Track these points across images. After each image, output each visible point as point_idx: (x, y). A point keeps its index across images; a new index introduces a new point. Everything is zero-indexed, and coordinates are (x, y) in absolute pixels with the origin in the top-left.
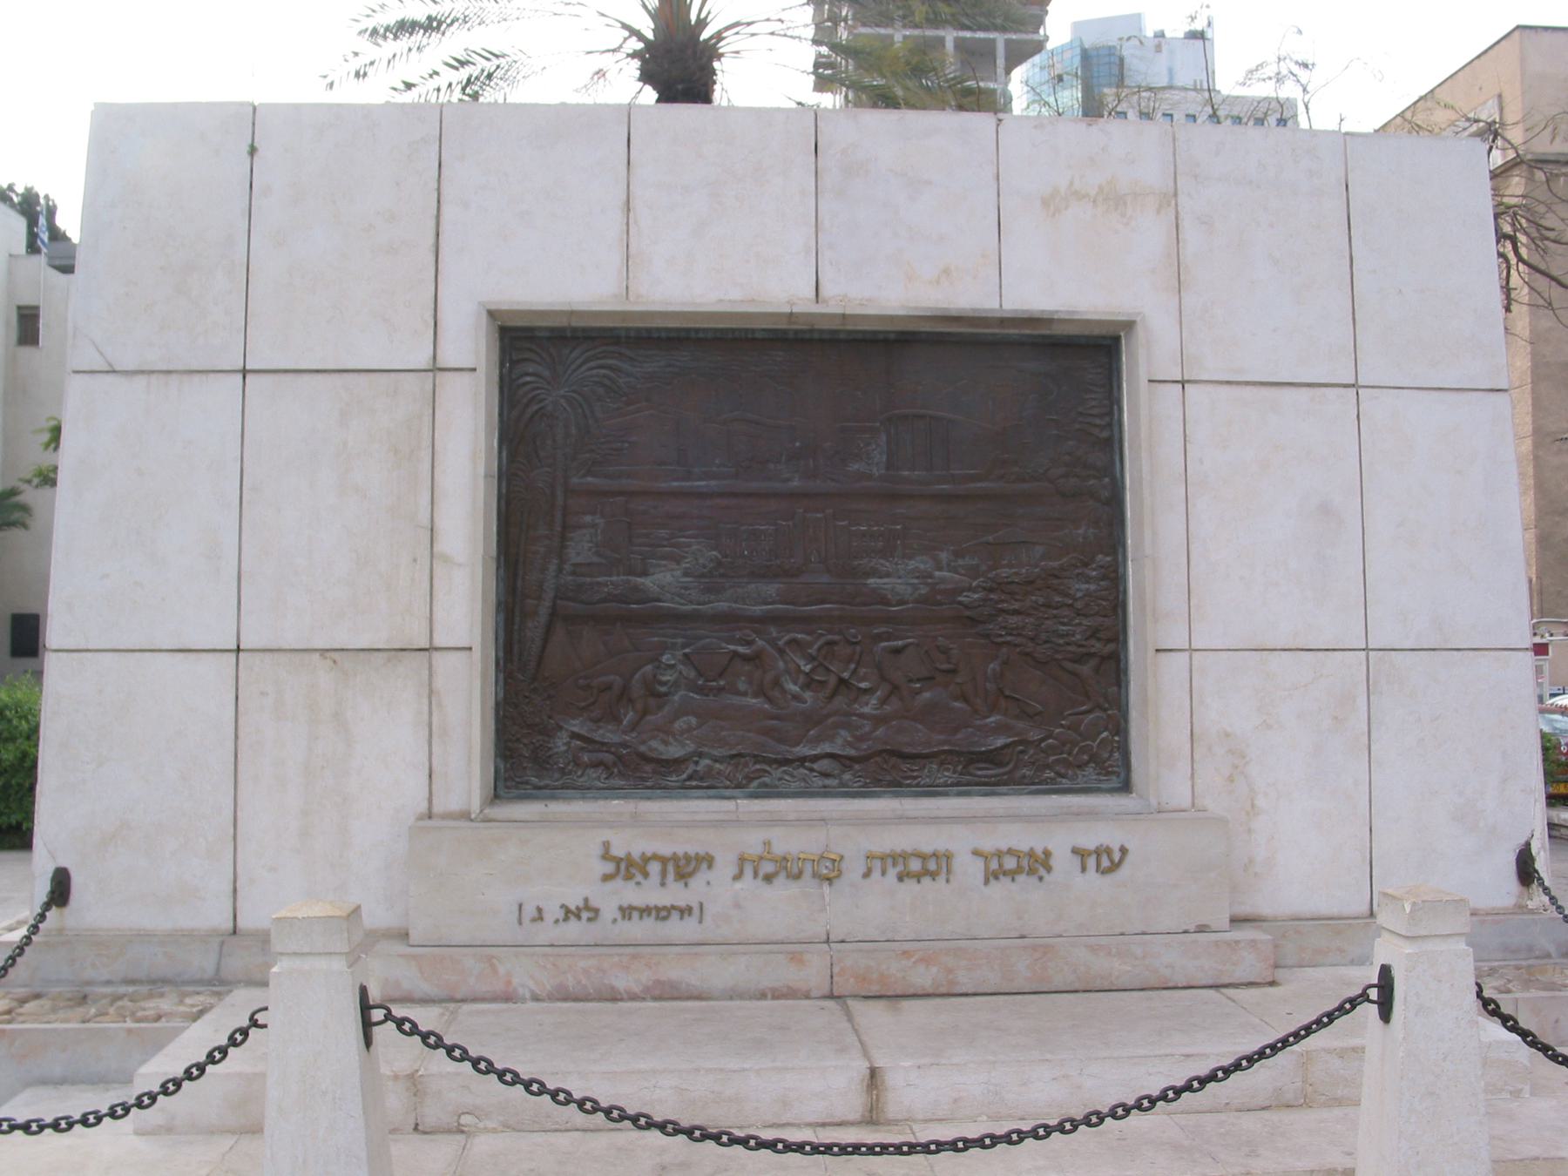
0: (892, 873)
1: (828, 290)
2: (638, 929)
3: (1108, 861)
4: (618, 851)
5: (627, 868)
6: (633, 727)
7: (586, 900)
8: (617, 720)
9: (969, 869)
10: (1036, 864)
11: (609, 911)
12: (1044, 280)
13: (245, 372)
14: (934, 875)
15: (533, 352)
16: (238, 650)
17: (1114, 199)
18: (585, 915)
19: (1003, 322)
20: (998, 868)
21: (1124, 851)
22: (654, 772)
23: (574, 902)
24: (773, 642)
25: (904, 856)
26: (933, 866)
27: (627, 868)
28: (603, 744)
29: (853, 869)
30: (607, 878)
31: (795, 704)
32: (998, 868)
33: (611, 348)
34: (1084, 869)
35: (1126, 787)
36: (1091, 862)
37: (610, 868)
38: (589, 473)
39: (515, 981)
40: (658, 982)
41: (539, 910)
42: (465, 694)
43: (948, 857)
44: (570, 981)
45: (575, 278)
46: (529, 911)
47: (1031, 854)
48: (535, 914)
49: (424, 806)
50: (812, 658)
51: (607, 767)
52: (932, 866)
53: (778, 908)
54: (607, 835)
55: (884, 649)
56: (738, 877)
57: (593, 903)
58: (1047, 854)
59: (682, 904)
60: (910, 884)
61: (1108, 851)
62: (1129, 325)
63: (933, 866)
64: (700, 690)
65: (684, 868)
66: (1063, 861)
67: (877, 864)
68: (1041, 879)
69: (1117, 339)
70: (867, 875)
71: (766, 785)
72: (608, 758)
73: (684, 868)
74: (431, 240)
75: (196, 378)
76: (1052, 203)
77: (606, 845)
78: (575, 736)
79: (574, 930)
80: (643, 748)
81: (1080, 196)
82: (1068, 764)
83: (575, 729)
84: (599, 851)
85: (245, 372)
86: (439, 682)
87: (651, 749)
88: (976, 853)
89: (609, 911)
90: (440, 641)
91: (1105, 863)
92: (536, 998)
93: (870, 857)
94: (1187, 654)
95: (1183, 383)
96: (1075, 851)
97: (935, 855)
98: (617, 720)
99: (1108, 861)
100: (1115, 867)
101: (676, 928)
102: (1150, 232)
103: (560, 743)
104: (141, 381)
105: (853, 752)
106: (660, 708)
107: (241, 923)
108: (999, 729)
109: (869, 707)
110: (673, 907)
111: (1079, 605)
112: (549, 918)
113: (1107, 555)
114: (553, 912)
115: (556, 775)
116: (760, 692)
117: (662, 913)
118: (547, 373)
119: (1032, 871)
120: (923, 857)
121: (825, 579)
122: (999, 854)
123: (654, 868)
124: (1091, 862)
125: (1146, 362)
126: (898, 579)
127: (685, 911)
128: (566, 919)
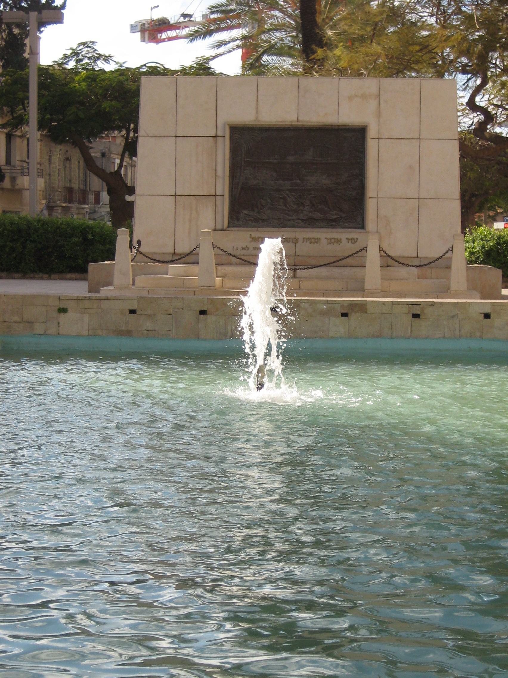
0: (308, 242)
1: (300, 119)
3: (354, 241)
4: (253, 236)
8: (254, 211)
9: (324, 242)
10: (338, 241)
11: (251, 249)
12: (348, 116)
13: (176, 136)
14: (316, 242)
16: (175, 195)
17: (364, 97)
19: (338, 126)
20: (331, 241)
21: (357, 239)
23: (244, 246)
24: (287, 195)
25: (311, 239)
26: (317, 241)
29: (300, 241)
30: (251, 242)
32: (331, 241)
36: (350, 241)
37: (251, 239)
43: (320, 239)
45: (246, 116)
46: (235, 248)
47: (337, 239)
49: (214, 228)
50: (296, 198)
52: (316, 240)
54: (251, 233)
57: (248, 246)
58: (341, 239)
60: (312, 244)
61: (354, 239)
62: (367, 126)
63: (317, 241)
66: (344, 241)
67: (305, 240)
70: (303, 242)
72: (253, 219)
74: (215, 108)
75: (166, 138)
76: (350, 98)
81: (356, 96)
82: (350, 222)
84: (249, 236)
85: (176, 136)
86: (218, 203)
88: (326, 238)
89: (251, 249)
90: (217, 194)
91: (353, 241)
93: (304, 238)
94: (376, 199)
95: (378, 139)
96: (347, 239)
97: (317, 239)
98: (254, 211)
99: (354, 241)
100: (355, 242)
102: (373, 104)
103: (242, 215)
104: (154, 138)
112: (239, 250)
114: (240, 248)
116: (285, 205)
119: (337, 243)
120: (315, 239)
121: (299, 181)
122: (331, 239)
124: (350, 241)
125: (372, 133)
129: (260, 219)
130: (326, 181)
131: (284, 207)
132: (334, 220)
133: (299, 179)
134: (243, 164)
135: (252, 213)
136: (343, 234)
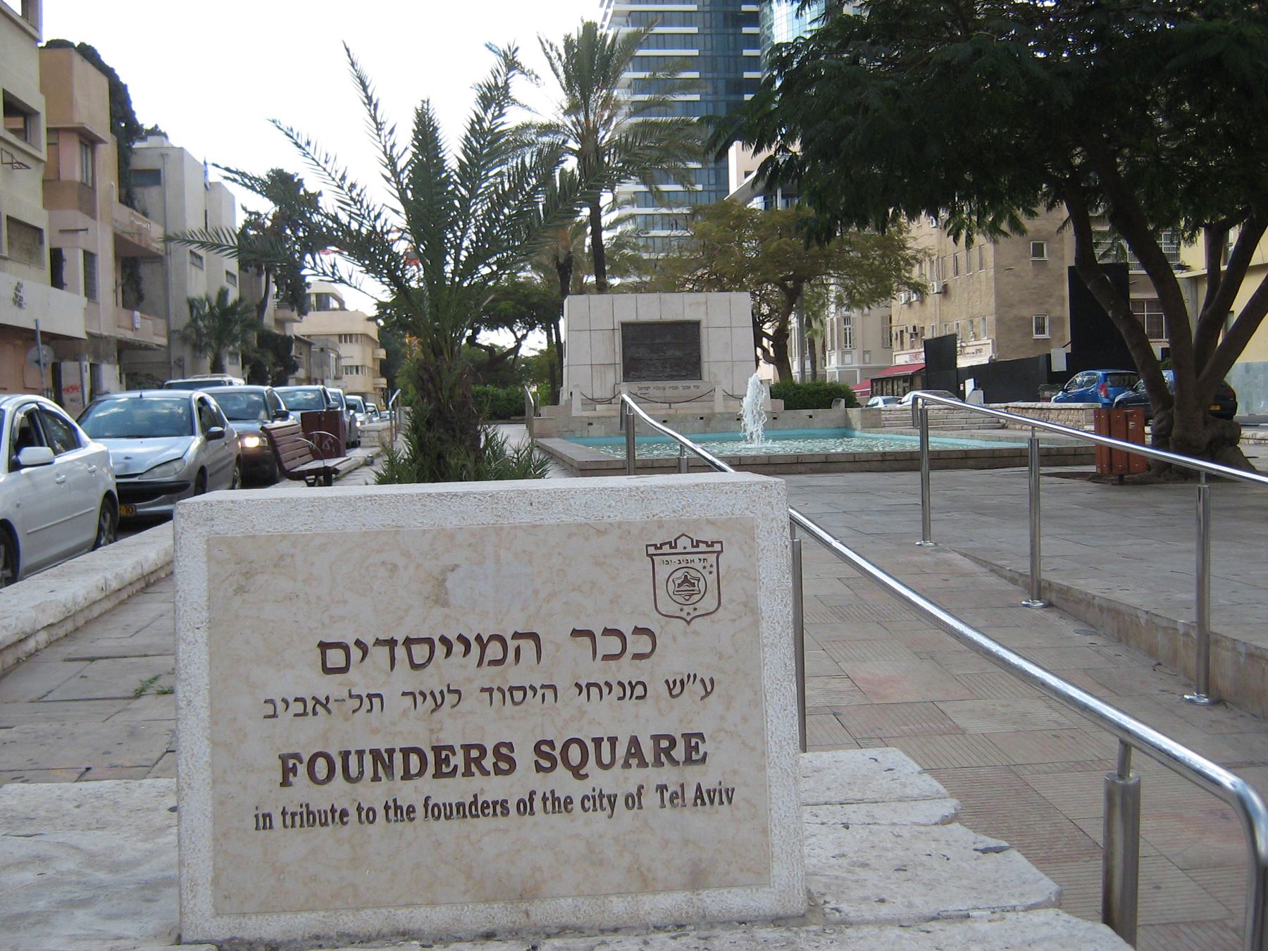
12: (689, 316)
15: (625, 326)
17: (698, 304)
20: (684, 388)
26: (676, 388)
32: (684, 388)
45: (630, 317)
53: (658, 393)
63: (676, 388)
65: (647, 388)
73: (647, 388)
102: (703, 309)
125: (703, 324)
126: (669, 353)
130: (678, 353)
136: (691, 383)
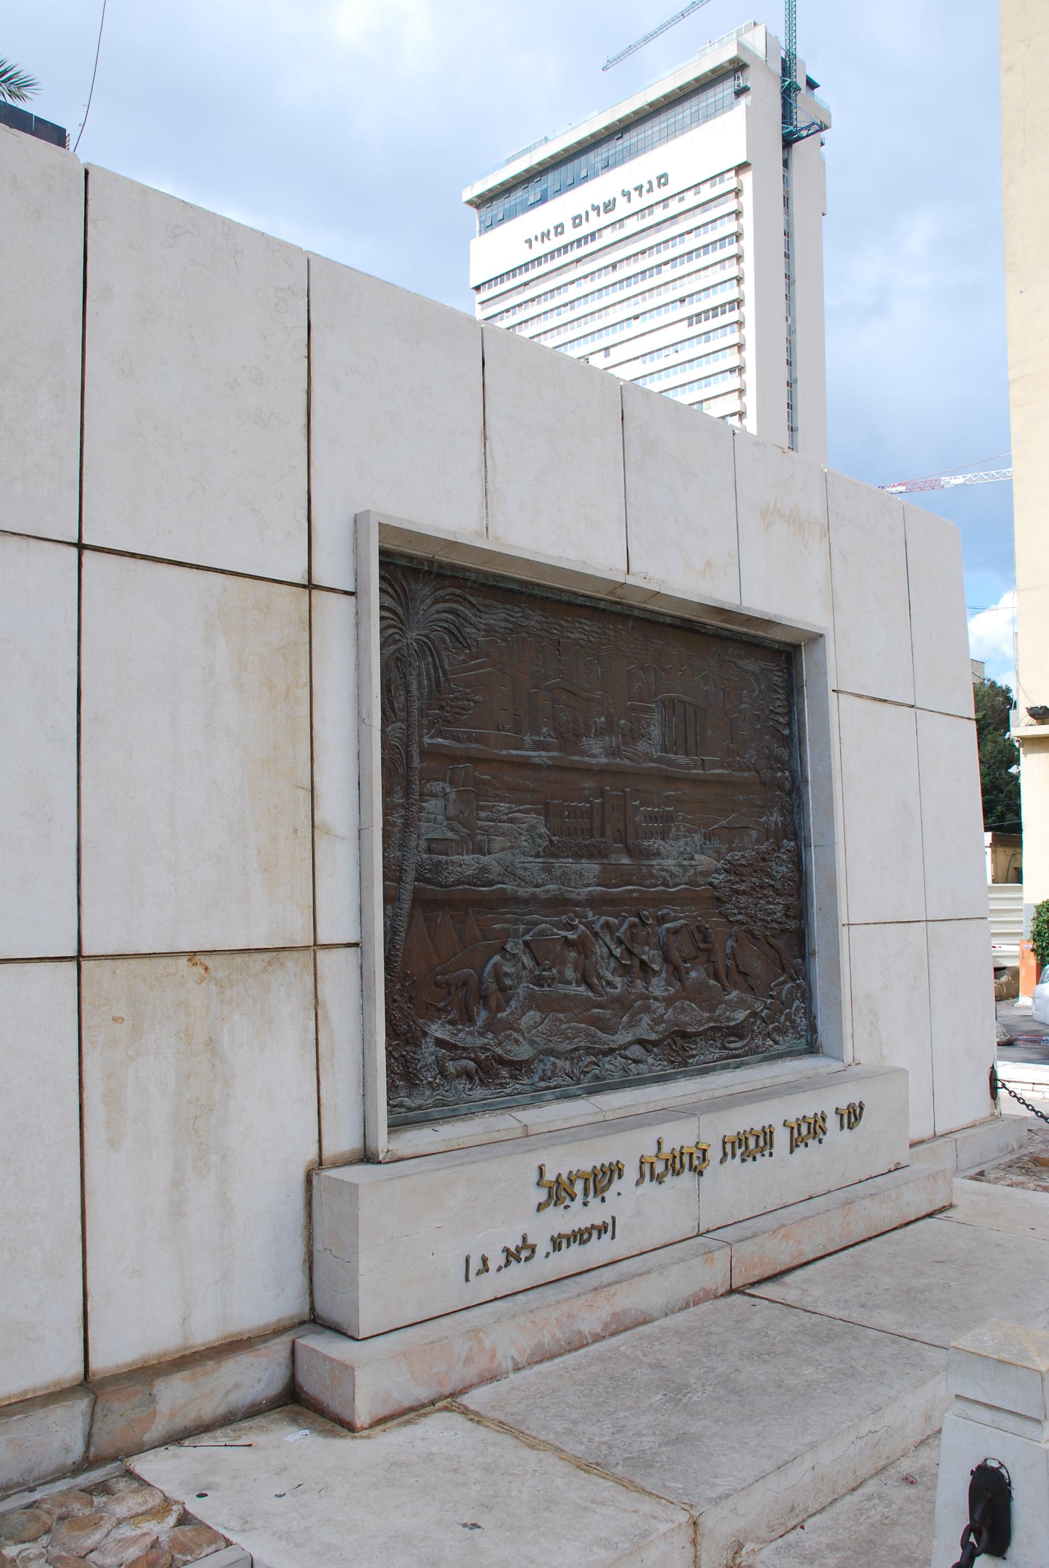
2: (572, 1257)
5: (558, 1192)
6: (490, 1026)
7: (524, 1238)
8: (471, 1020)
13: (81, 546)
18: (524, 1254)
22: (513, 1077)
27: (558, 1192)
28: (464, 1049)
29: (714, 1154)
31: (608, 989)
33: (457, 591)
34: (842, 1127)
35: (813, 1049)
38: (440, 734)
39: (499, 1354)
40: (615, 1315)
41: (484, 1260)
42: (352, 1002)
44: (547, 1338)
46: (476, 1264)
48: (480, 1266)
51: (470, 1077)
55: (668, 930)
56: (638, 1183)
59: (598, 1222)
62: (816, 638)
64: (539, 981)
65: (601, 1179)
68: (820, 1141)
69: (797, 648)
71: (597, 1078)
73: (601, 1179)
77: (541, 1169)
78: (440, 1043)
79: (519, 1275)
80: (499, 1051)
83: (438, 1035)
85: (81, 546)
87: (507, 1052)
89: (544, 1246)
92: (517, 1369)
100: (858, 1119)
101: (599, 1249)
105: (654, 1037)
106: (507, 1002)
107: (100, 1363)
108: (741, 1004)
109: (658, 987)
110: (593, 1227)
111: (778, 885)
113: (790, 840)
114: (496, 1259)
115: (428, 1093)
117: (581, 1237)
118: (400, 610)
121: (626, 861)
123: (578, 1187)
127: (602, 1229)
128: (508, 1263)
129: (501, 1061)
131: (582, 989)
132: (738, 1032)
133: (629, 853)
134: (416, 763)
135: (465, 1037)
